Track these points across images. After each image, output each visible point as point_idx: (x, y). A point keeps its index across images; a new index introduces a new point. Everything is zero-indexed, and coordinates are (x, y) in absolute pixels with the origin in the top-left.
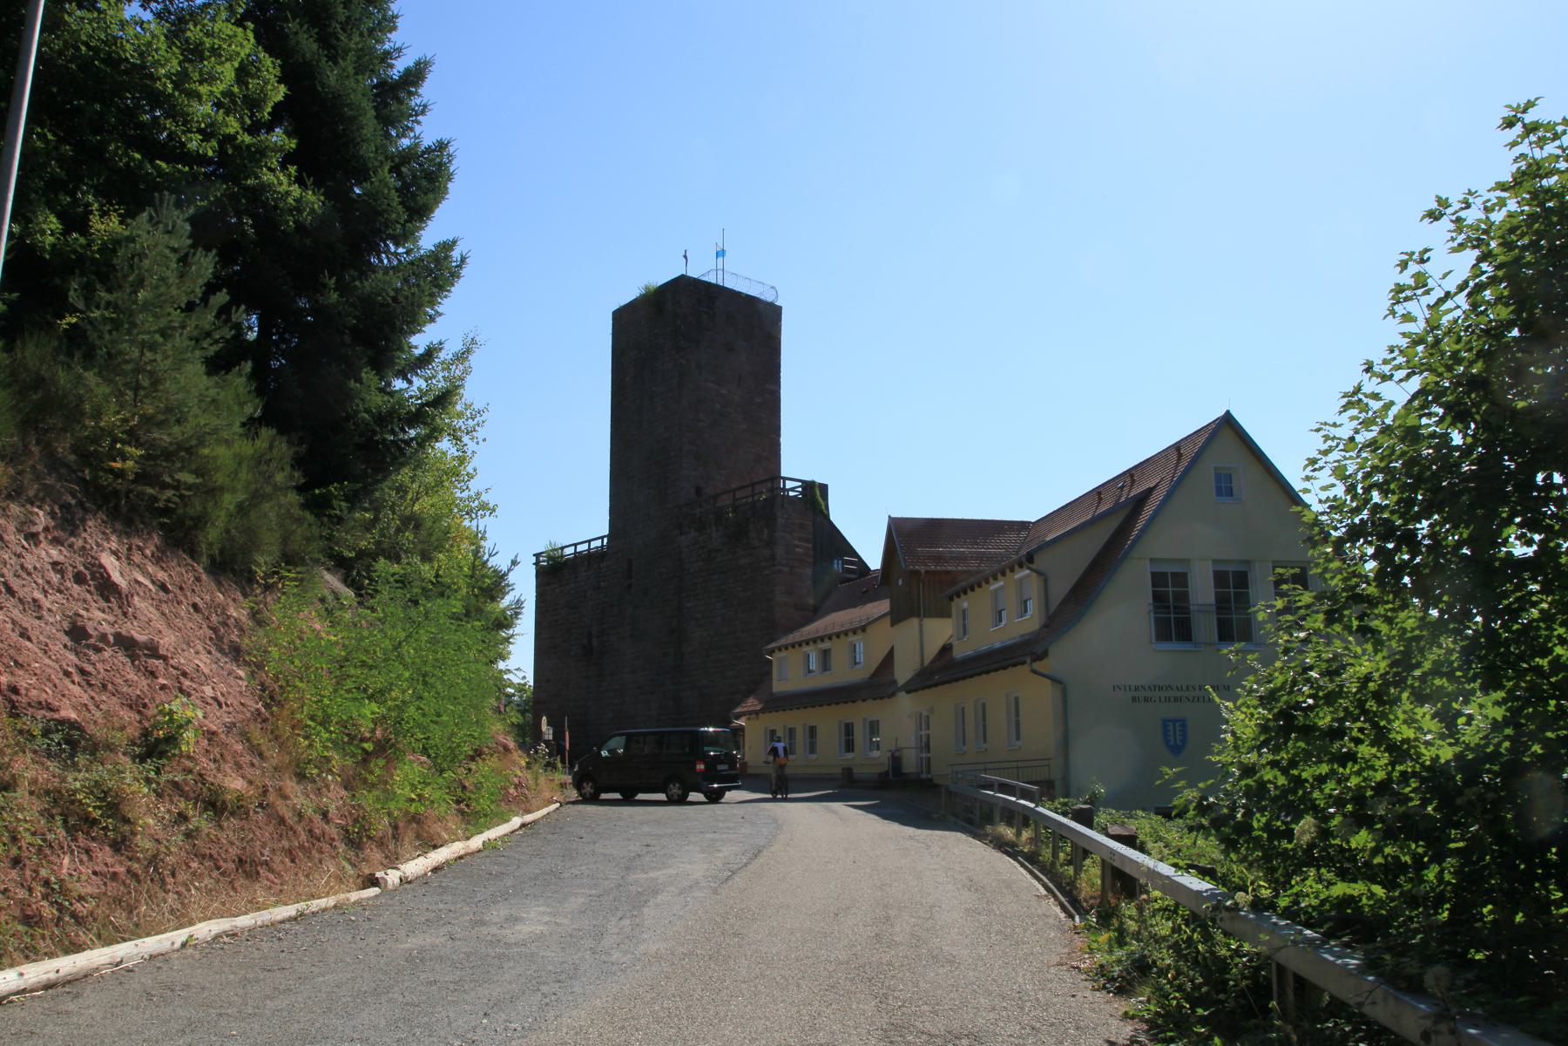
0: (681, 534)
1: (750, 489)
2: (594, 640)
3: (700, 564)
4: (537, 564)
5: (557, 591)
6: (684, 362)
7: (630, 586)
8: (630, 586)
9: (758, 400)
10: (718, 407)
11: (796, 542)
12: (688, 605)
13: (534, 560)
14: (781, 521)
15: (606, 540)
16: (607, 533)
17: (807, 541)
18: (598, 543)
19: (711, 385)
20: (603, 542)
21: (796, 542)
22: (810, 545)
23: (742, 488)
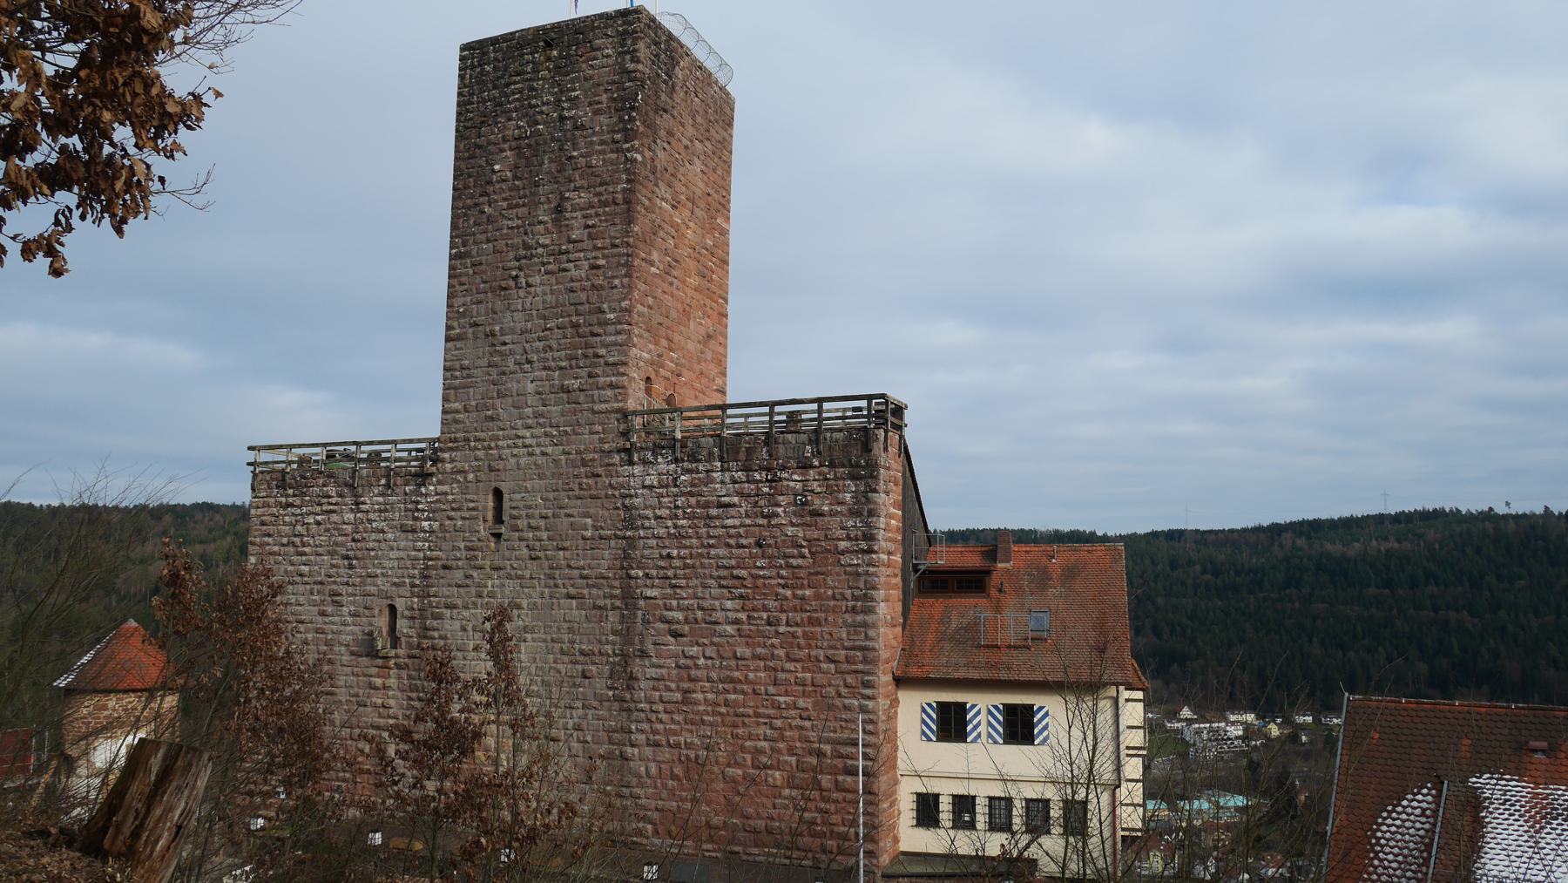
6: (639, 157)
12: (649, 593)
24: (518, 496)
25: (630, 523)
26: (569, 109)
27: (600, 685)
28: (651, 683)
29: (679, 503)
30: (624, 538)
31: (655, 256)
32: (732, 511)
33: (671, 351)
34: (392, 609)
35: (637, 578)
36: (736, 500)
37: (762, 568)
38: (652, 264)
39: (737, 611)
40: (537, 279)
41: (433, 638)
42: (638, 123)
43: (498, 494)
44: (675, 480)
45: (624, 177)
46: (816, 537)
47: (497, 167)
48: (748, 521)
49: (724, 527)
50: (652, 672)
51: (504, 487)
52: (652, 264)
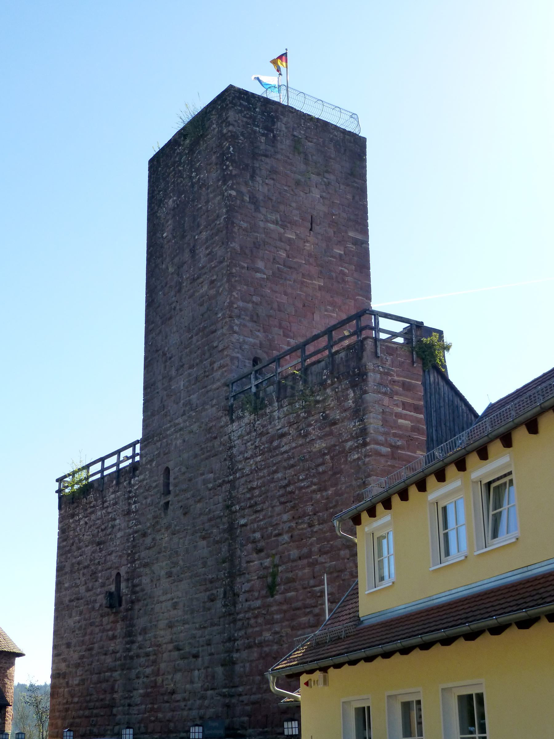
0: (232, 421)
1: (326, 338)
2: (123, 585)
3: (259, 459)
4: (59, 491)
5: (82, 522)
7: (167, 504)
8: (167, 504)
9: (339, 251)
10: (283, 254)
11: (400, 410)
12: (243, 522)
13: (56, 486)
14: (373, 378)
15: (138, 447)
16: (139, 436)
17: (416, 409)
18: (129, 452)
19: (272, 226)
20: (134, 450)
21: (400, 410)
22: (422, 416)
23: (316, 337)
24: (177, 469)
25: (232, 470)
26: (197, 175)
27: (219, 604)
28: (247, 595)
29: (257, 444)
30: (229, 482)
31: (260, 264)
32: (285, 440)
33: (287, 337)
34: (118, 574)
35: (236, 512)
36: (286, 429)
37: (302, 480)
38: (258, 270)
39: (290, 521)
40: (185, 303)
41: (137, 592)
42: (231, 168)
43: (167, 470)
44: (254, 426)
45: (224, 211)
46: (332, 443)
47: (165, 235)
48: (294, 445)
49: (282, 454)
50: (246, 587)
51: (171, 465)
52: (258, 270)
